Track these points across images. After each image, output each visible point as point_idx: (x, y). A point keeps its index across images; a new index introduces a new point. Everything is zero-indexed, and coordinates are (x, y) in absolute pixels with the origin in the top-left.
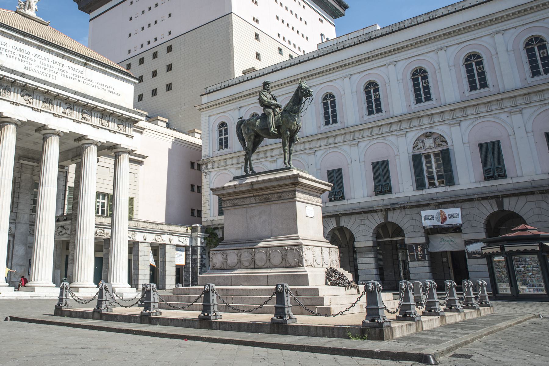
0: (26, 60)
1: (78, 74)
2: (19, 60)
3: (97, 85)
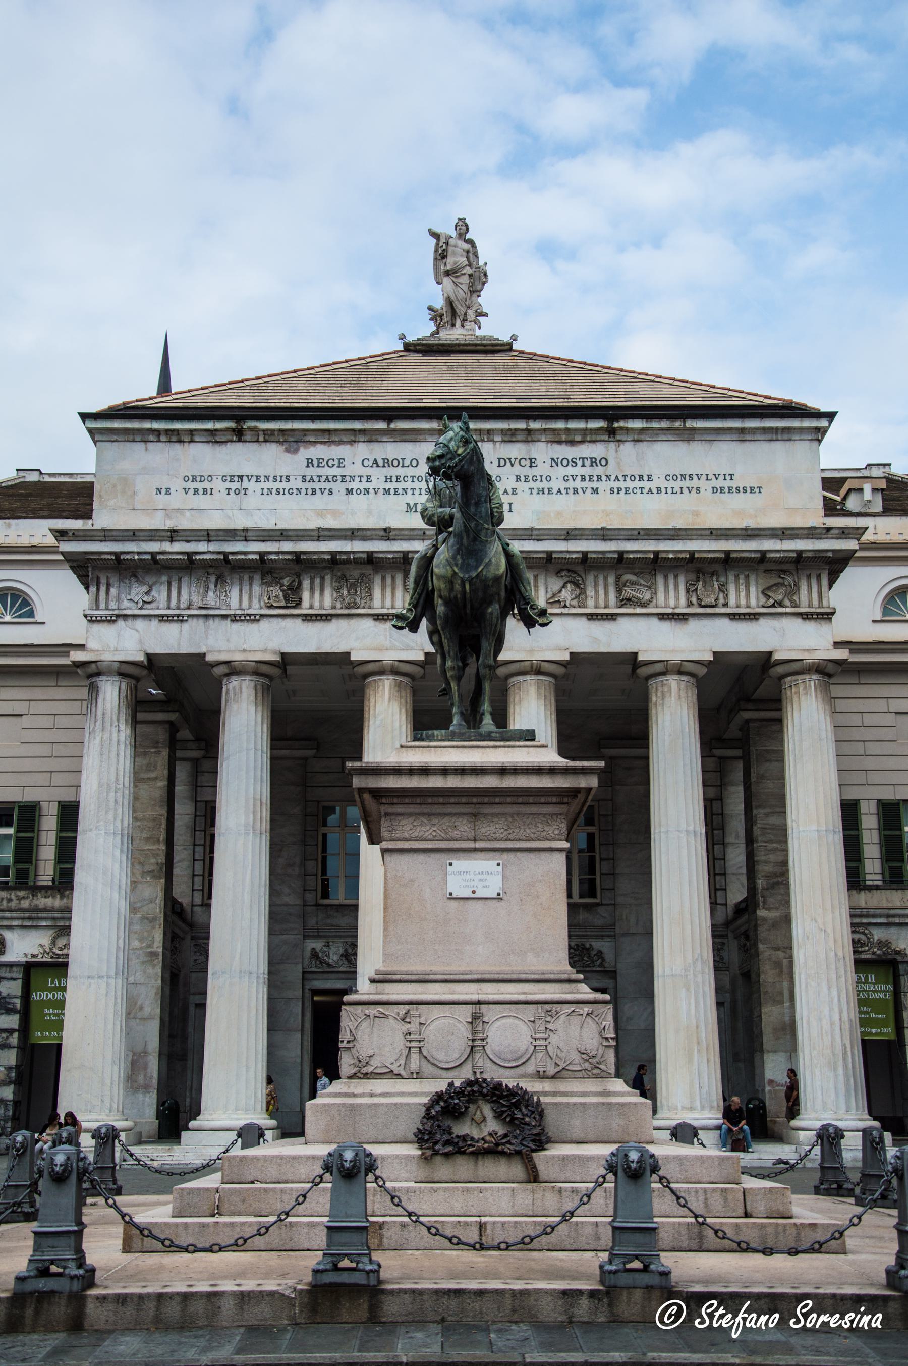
0: (409, 485)
1: (587, 471)
2: (387, 492)
3: (663, 484)
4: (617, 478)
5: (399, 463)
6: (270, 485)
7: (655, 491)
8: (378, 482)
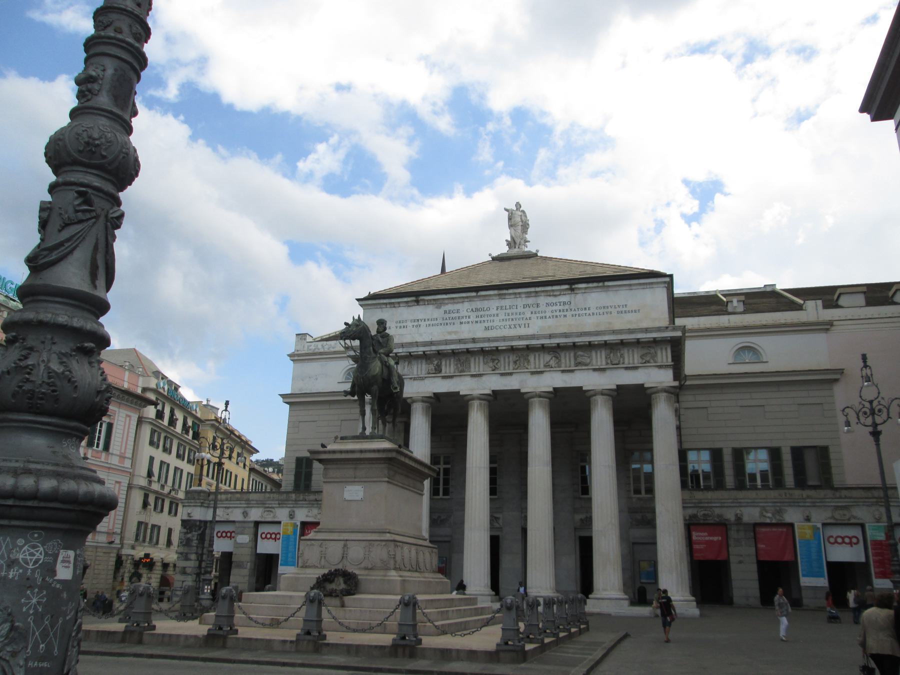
0: (486, 319)
1: (561, 308)
2: (477, 322)
5: (482, 309)
6: (431, 323)
8: (473, 319)
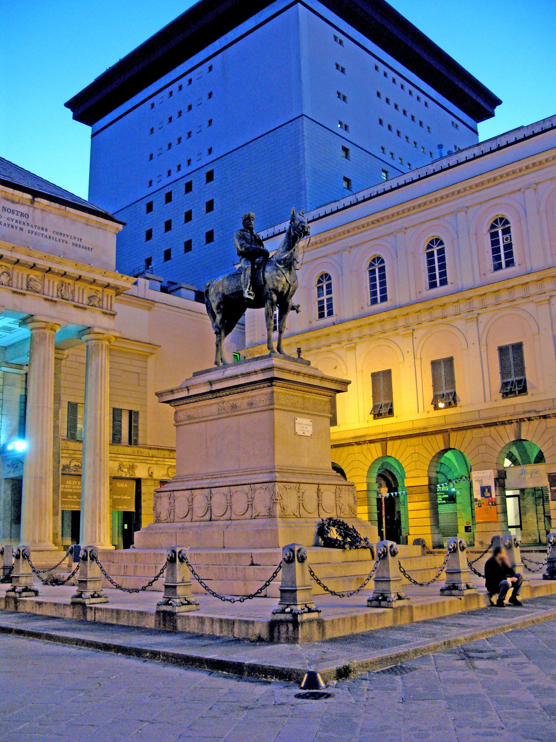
1: (18, 218)
4: (32, 226)
7: (48, 237)
